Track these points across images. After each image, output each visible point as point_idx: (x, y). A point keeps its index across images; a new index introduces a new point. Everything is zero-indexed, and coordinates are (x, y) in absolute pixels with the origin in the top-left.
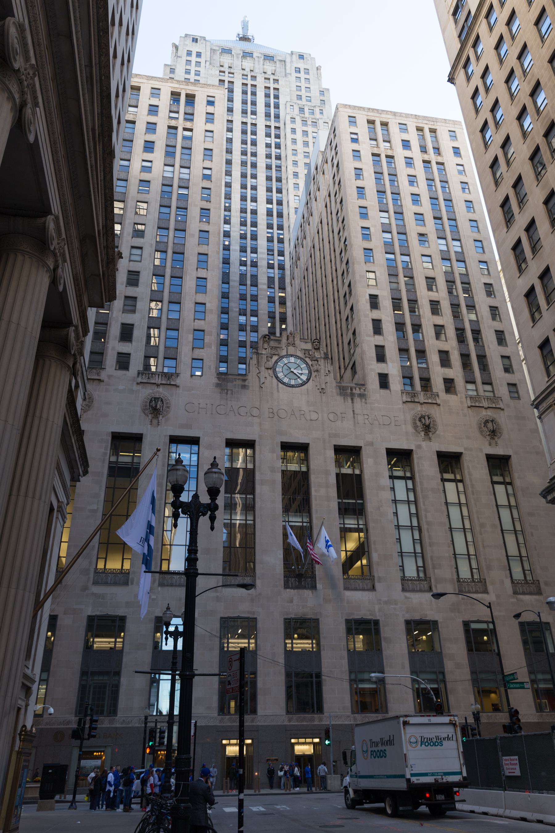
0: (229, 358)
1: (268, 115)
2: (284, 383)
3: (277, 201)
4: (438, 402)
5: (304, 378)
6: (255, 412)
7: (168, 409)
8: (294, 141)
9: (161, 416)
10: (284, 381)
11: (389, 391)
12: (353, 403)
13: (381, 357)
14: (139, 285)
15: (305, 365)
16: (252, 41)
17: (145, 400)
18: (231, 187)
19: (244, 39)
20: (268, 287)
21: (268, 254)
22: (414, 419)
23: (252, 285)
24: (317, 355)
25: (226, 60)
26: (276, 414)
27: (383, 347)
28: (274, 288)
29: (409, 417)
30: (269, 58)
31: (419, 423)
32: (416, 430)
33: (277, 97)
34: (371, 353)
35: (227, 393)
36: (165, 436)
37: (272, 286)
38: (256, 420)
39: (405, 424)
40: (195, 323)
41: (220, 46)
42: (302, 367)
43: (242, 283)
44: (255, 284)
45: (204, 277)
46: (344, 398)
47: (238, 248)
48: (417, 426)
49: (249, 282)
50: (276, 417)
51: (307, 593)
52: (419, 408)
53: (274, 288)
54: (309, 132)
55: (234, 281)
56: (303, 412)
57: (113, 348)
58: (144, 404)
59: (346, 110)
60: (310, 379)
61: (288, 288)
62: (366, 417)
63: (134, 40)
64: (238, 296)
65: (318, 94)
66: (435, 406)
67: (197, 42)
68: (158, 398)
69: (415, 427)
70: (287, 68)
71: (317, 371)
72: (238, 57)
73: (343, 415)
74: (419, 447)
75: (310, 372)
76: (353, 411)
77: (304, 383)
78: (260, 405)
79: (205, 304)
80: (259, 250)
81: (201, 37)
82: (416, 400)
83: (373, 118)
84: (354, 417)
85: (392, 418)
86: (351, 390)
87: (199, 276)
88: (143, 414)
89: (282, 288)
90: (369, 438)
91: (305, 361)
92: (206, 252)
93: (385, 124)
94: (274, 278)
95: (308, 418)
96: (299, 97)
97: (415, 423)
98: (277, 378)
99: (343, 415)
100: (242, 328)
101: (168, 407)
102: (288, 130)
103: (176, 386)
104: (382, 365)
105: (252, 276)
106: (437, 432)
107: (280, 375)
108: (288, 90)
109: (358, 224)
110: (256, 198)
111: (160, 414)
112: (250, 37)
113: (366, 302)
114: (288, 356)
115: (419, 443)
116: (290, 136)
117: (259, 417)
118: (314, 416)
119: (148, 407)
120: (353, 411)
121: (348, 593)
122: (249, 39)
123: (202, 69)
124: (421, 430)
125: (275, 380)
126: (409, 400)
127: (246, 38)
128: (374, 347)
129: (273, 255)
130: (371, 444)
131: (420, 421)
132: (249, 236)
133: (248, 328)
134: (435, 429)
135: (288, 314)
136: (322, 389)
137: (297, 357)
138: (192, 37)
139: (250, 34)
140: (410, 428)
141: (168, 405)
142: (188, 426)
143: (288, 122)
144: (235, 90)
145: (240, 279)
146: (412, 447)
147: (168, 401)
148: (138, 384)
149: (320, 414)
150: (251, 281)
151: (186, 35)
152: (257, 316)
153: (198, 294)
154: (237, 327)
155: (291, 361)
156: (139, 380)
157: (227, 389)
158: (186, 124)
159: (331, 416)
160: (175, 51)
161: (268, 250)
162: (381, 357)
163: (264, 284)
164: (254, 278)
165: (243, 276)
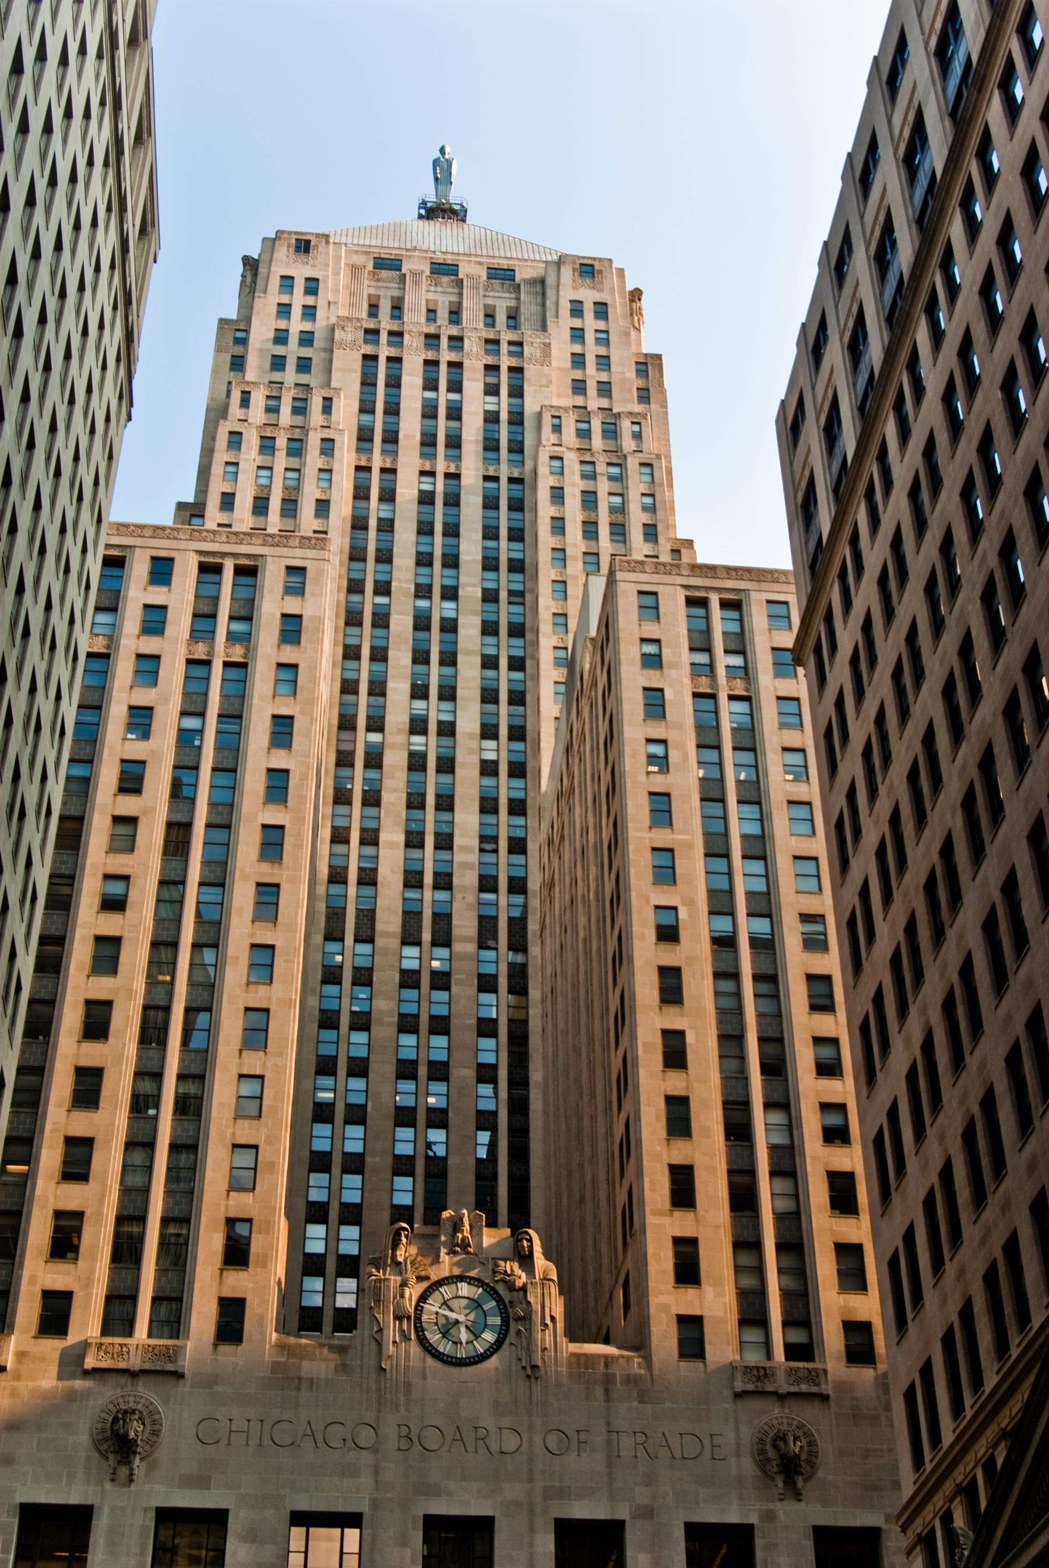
0: (369, 1159)
1: (491, 445)
2: (438, 1356)
3: (511, 692)
4: (827, 1388)
5: (489, 1337)
6: (366, 1436)
7: (154, 1438)
8: (559, 525)
9: (138, 1457)
10: (441, 1349)
11: (701, 1365)
12: (608, 1400)
13: (687, 1272)
14: (101, 1105)
15: (493, 1303)
16: (462, 214)
17: (103, 1415)
18: (385, 659)
20: (480, 947)
21: (481, 850)
22: (761, 1441)
23: (435, 944)
26: (415, 1440)
27: (693, 1242)
28: (496, 949)
29: (747, 1435)
31: (771, 1453)
32: (765, 1473)
33: (517, 392)
34: (661, 1263)
35: (298, 1389)
36: (146, 1510)
37: (491, 943)
38: (367, 1458)
39: (738, 1455)
40: (231, 1202)
41: (367, 253)
42: (486, 1307)
43: (410, 937)
44: (443, 938)
45: (258, 1073)
46: (587, 1388)
47: (401, 838)
48: (768, 1460)
49: (427, 936)
50: (417, 1447)
52: (775, 1411)
53: (496, 949)
54: (599, 494)
55: (387, 935)
56: (482, 1433)
57: (33, 1280)
58: (99, 1426)
59: (632, 576)
60: (504, 1339)
61: (534, 950)
62: (640, 1438)
63: (113, 469)
64: (397, 977)
65: (631, 373)
66: (817, 1403)
68: (133, 1412)
69: (762, 1463)
70: (548, 303)
71: (523, 1318)
72: (416, 283)
73: (583, 1437)
74: (769, 1516)
75: (506, 1322)
76: (608, 1424)
78: (378, 1418)
79: (256, 1147)
80: (457, 841)
81: (318, 235)
82: (770, 1388)
83: (702, 594)
84: (609, 1442)
85: (707, 1441)
86: (607, 1365)
87: (245, 1072)
88: (96, 1454)
89: (518, 943)
90: (643, 1496)
91: (496, 1292)
92: (265, 1006)
93: (733, 605)
94: (495, 918)
95: (495, 1447)
96: (579, 387)
97: (762, 1452)
98: (423, 1341)
99: (583, 1437)
100: (406, 1070)
101: (156, 1433)
102: (543, 494)
103: (179, 1375)
105: (435, 916)
106: (820, 1474)
109: (647, 900)
110: (454, 688)
111: (135, 1453)
112: (457, 207)
113: (658, 1119)
115: (771, 1506)
116: (546, 510)
117: (374, 1450)
118: (511, 1442)
119: (109, 1433)
120: (608, 1424)
122: (454, 212)
124: (775, 1469)
125: (415, 1348)
126: (750, 1387)
127: (444, 211)
128: (670, 1244)
129: (496, 851)
130: (647, 1513)
131: (775, 1446)
132: (430, 801)
133: (423, 1071)
134: (812, 1465)
135: (531, 1023)
136: (535, 1367)
138: (294, 237)
139: (455, 196)
140: (748, 1467)
141: (156, 1427)
142: (201, 1482)
143: (543, 470)
144: (405, 380)
145: (404, 926)
146: (753, 1519)
147: (157, 1417)
148: (87, 1373)
149: (524, 1437)
150: (434, 932)
151: (279, 234)
152: (446, 1032)
153: (240, 1121)
154: (391, 1069)
155: (460, 1293)
157: (300, 1379)
158: (231, 651)
159: (553, 1441)
160: (249, 279)
161: (483, 838)
163: (467, 939)
164: (443, 920)
165: (411, 918)
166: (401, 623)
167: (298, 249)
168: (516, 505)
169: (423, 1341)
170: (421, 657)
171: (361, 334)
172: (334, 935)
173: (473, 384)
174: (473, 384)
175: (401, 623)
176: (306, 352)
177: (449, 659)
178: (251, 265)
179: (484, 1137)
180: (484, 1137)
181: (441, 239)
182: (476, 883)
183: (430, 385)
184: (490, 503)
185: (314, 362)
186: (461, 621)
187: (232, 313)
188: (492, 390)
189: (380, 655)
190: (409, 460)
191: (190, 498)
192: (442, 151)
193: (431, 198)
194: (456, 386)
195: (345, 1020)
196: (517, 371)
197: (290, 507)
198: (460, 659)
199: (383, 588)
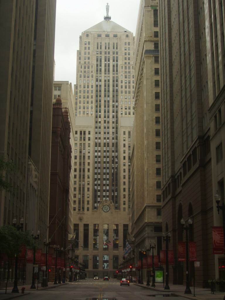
13: (124, 204)
19: (107, 18)
23: (107, 147)
24: (111, 205)
25: (99, 40)
30: (115, 36)
33: (117, 61)
43: (105, 146)
47: (103, 133)
51: (107, 251)
67: (88, 36)
77: (109, 211)
96: (126, 59)
98: (103, 210)
103: (84, 214)
104: (124, 206)
107: (104, 210)
108: (121, 57)
114: (105, 205)
121: (114, 251)
123: (90, 51)
125: (103, 211)
137: (107, 205)
139: (110, 15)
143: (120, 77)
144: (102, 60)
156: (78, 213)
162: (124, 204)
165: (105, 144)
166: (103, 102)
167: (87, 36)
168: (117, 81)
169: (103, 210)
170: (105, 107)
171: (96, 53)
172: (96, 146)
173: (111, 61)
174: (111, 61)
175: (103, 102)
176: (89, 56)
177: (108, 107)
178: (81, 37)
179: (113, 170)
180: (113, 170)
181: (107, 28)
182: (112, 139)
183: (105, 61)
184: (114, 81)
185: (90, 57)
186: (110, 101)
187: (78, 49)
188: (114, 61)
189: (100, 107)
190: (103, 74)
191: (76, 84)
192: (108, 4)
193: (106, 15)
194: (109, 61)
195: (98, 157)
196: (117, 57)
197: (88, 87)
198: (110, 107)
199: (100, 96)
